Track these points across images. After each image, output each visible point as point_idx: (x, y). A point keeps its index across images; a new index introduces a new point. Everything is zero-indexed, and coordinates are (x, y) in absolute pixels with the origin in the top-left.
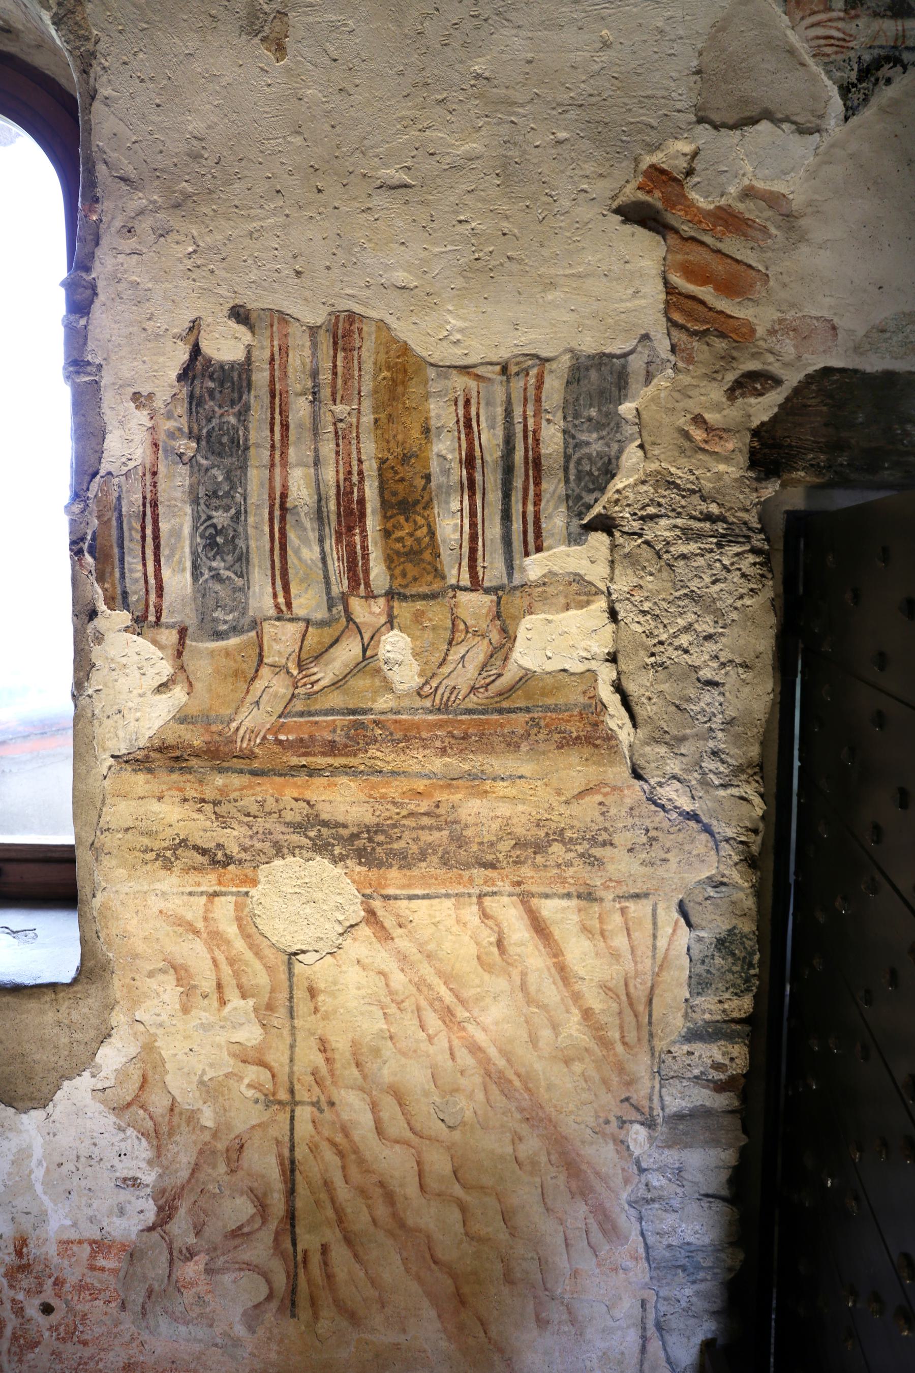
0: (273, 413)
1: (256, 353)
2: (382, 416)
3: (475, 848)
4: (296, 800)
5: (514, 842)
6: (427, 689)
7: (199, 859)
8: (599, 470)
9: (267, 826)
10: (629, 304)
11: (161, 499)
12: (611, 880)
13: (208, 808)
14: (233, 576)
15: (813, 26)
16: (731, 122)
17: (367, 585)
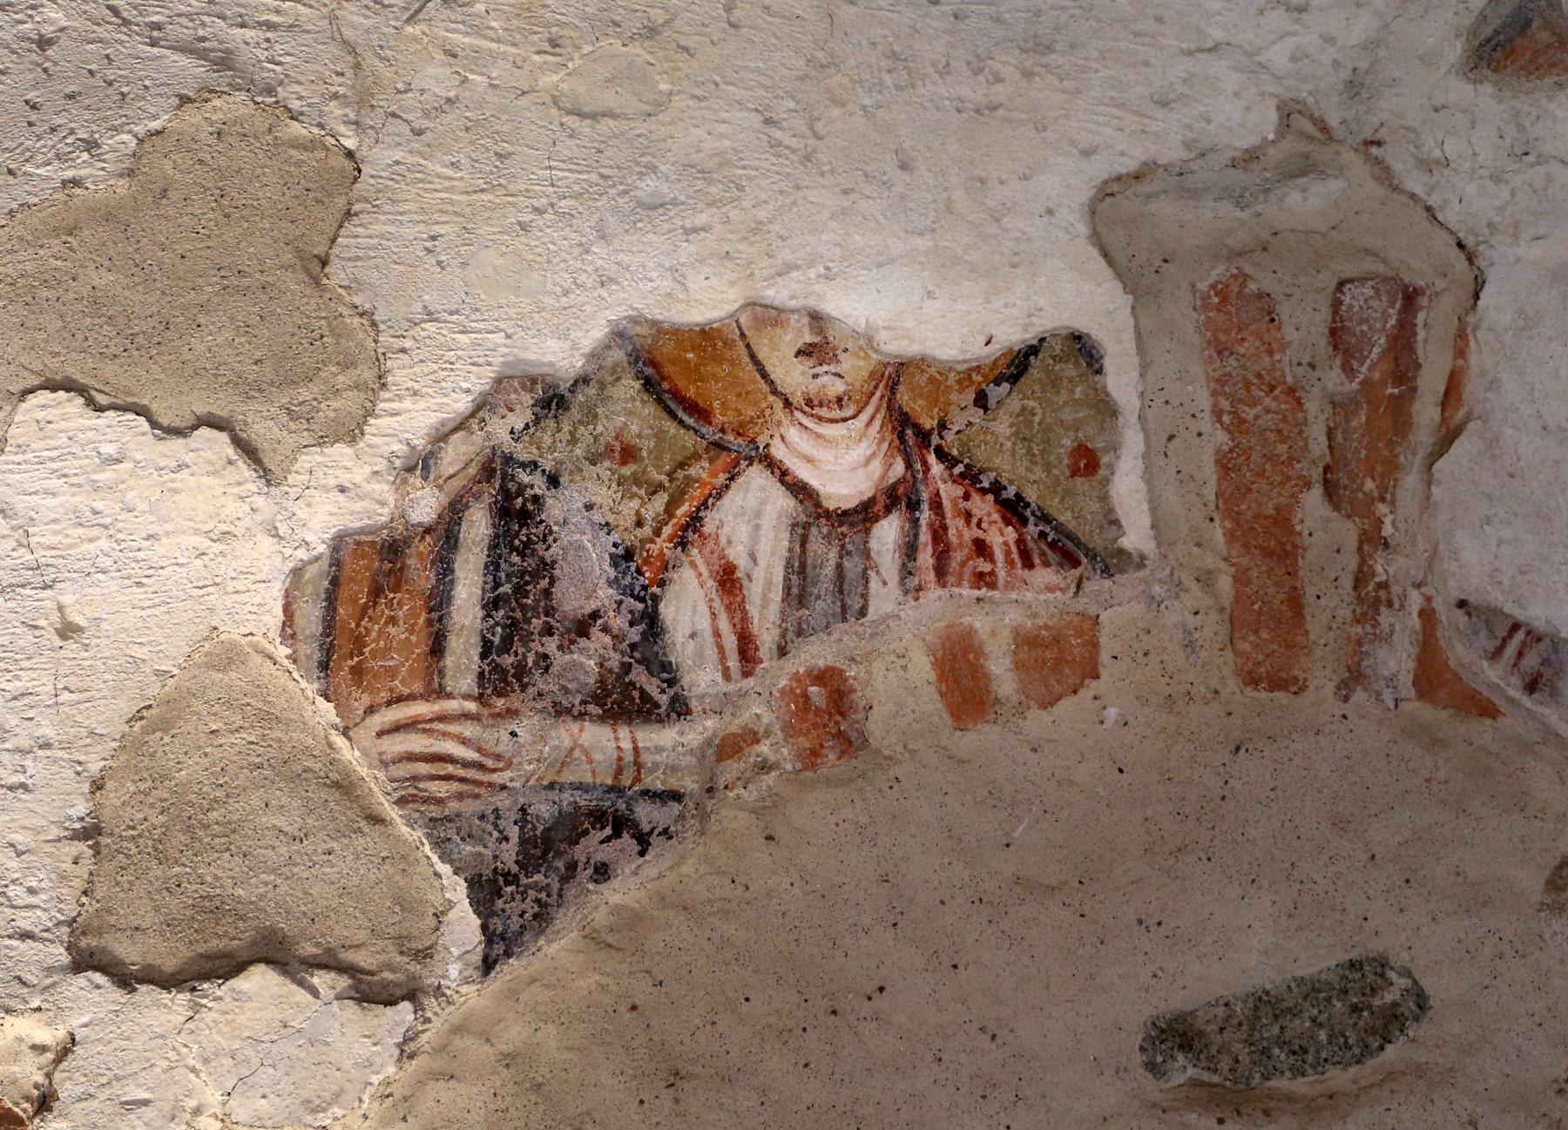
15: (396, 728)
16: (170, 965)
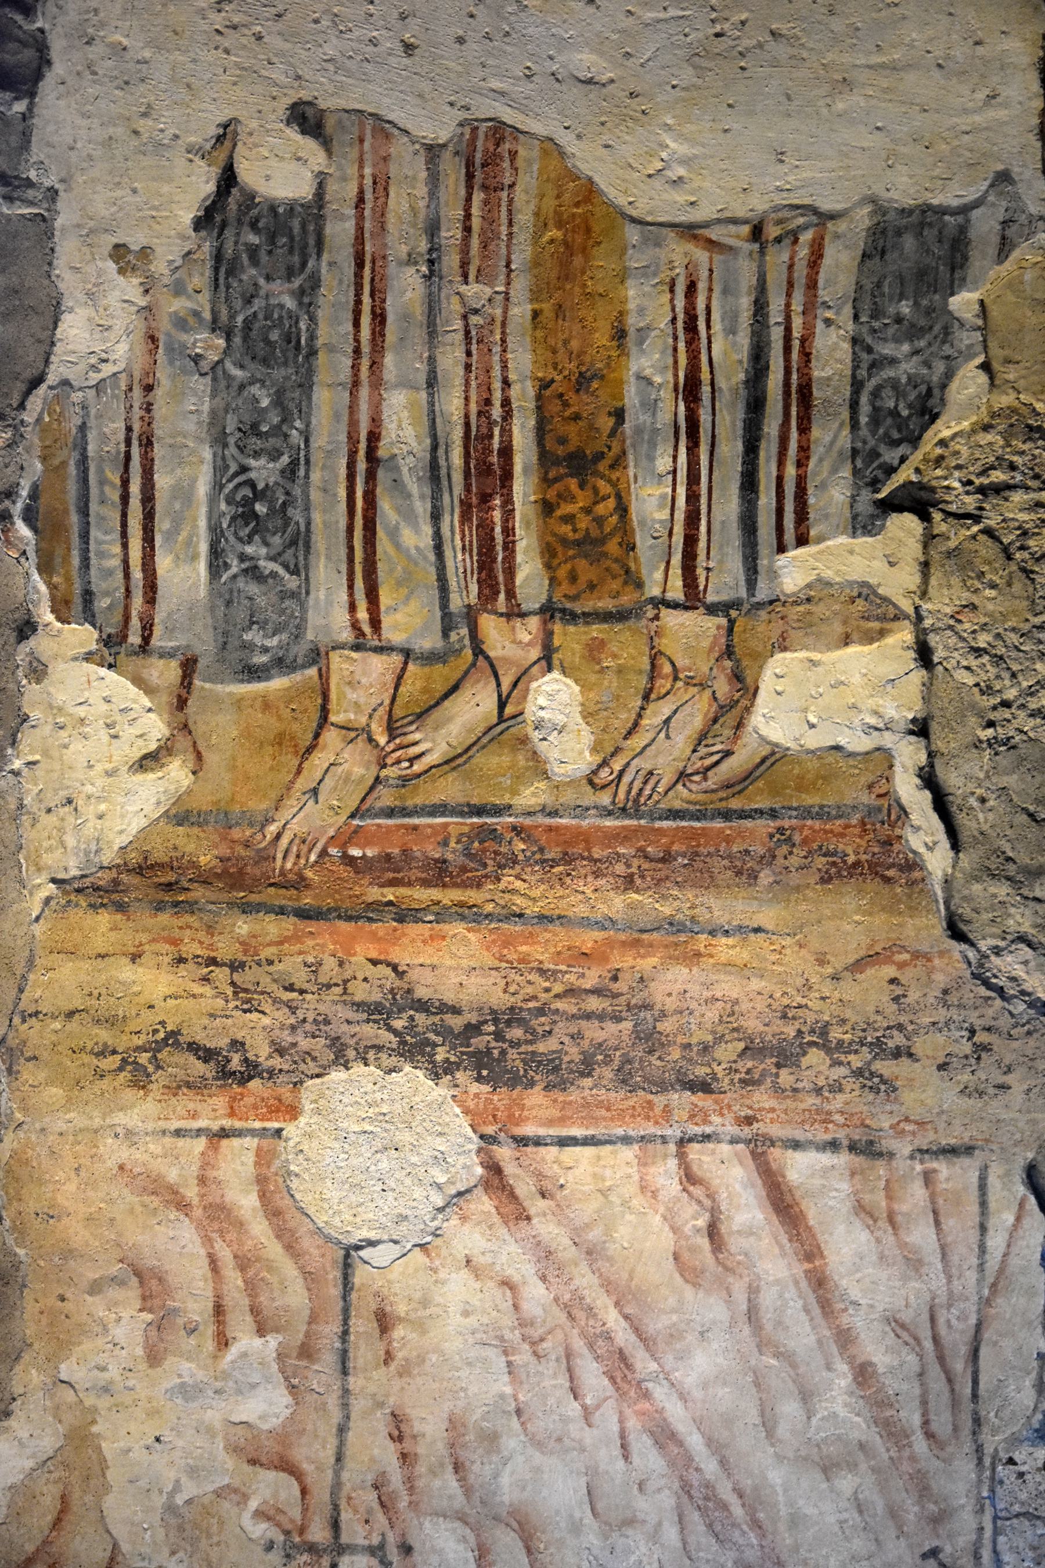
0: (358, 294)
1: (332, 188)
2: (547, 307)
3: (676, 1054)
4: (375, 962)
5: (741, 1045)
6: (604, 773)
7: (199, 1068)
8: (910, 406)
9: (322, 1008)
10: (977, 118)
11: (158, 432)
12: (907, 1119)
13: (221, 974)
14: (281, 571)
17: (511, 594)
